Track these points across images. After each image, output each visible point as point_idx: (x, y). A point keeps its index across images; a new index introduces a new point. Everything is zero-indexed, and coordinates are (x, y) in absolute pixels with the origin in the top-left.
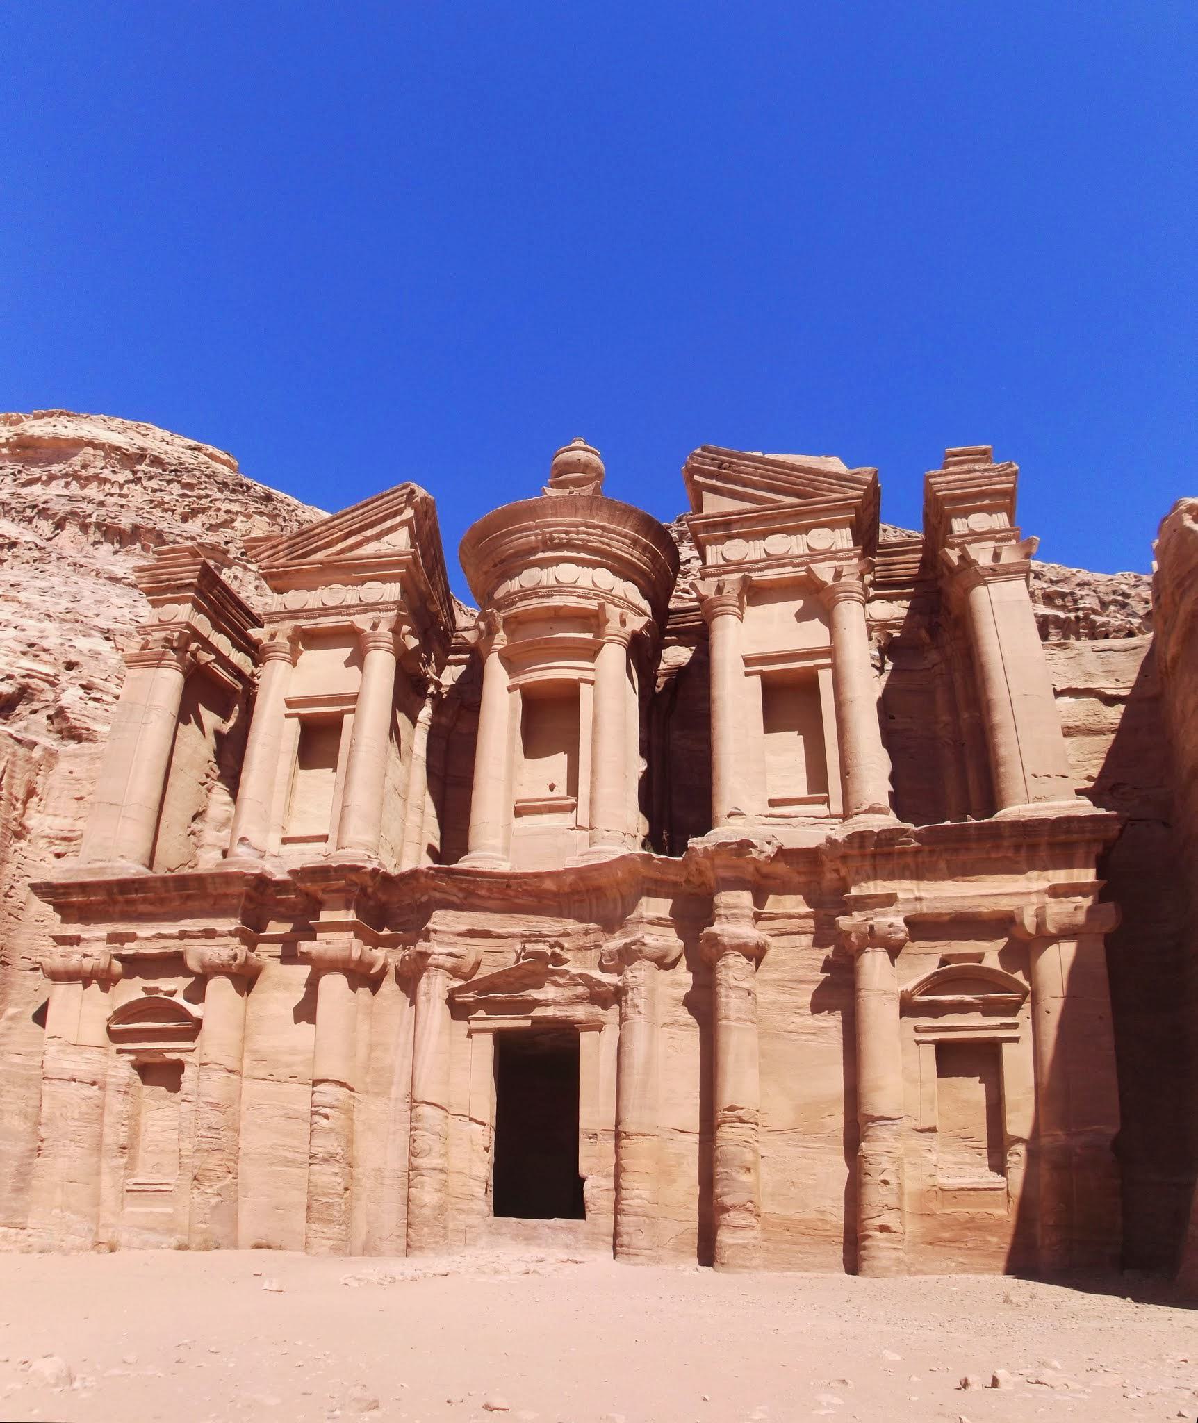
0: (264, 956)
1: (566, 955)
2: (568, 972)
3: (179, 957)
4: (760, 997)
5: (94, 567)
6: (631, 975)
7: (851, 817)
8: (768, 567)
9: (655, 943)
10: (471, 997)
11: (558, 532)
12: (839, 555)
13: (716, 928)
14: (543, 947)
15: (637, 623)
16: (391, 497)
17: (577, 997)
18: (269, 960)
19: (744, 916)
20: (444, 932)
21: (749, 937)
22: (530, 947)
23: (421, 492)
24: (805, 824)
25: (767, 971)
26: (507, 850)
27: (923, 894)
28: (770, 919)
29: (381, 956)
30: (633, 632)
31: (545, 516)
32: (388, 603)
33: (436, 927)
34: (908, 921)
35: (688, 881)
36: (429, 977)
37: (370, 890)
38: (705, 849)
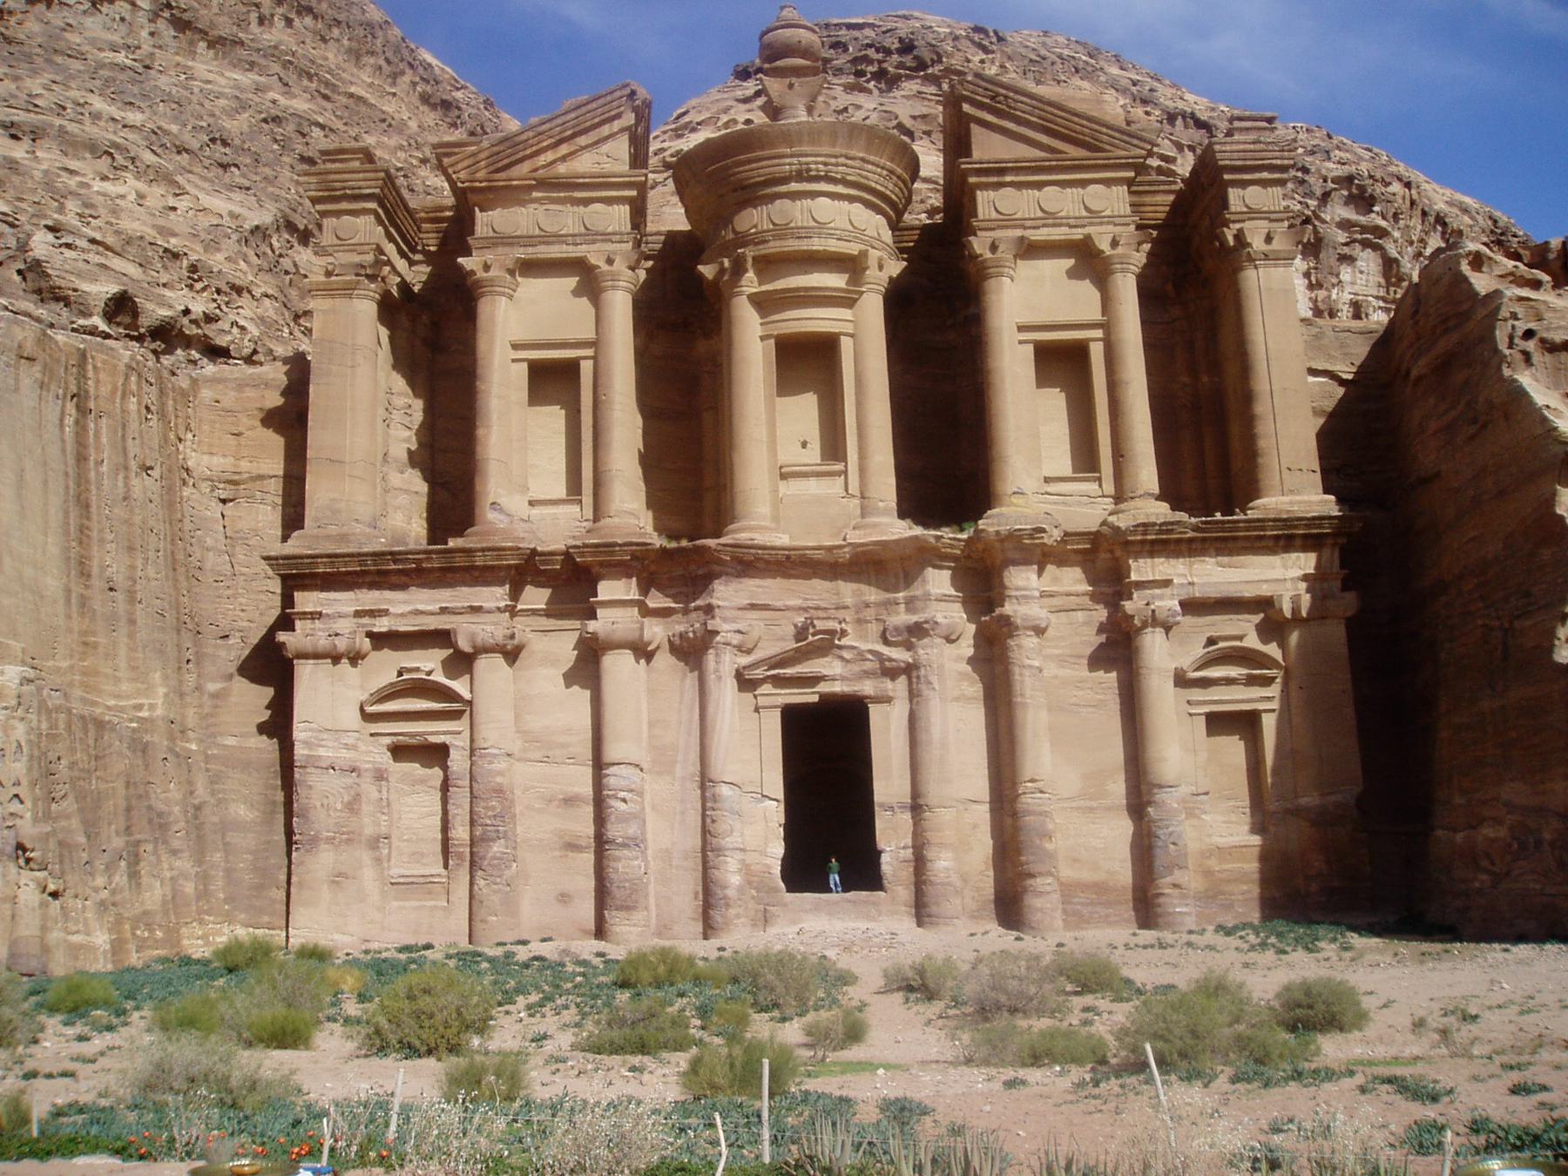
1: (849, 628)
2: (853, 648)
3: (441, 638)
4: (1046, 673)
7: (1126, 500)
8: (1044, 226)
10: (759, 673)
11: (816, 163)
12: (1117, 220)
13: (1008, 608)
15: (896, 267)
16: (609, 98)
17: (865, 672)
18: (530, 636)
19: (1033, 597)
20: (723, 607)
21: (1039, 619)
22: (820, 625)
23: (642, 93)
24: (1080, 504)
26: (776, 519)
27: (1195, 580)
29: (656, 632)
30: (891, 278)
31: (800, 143)
32: (621, 234)
33: (720, 603)
34: (1183, 604)
35: (968, 557)
36: (717, 655)
38: (998, 533)
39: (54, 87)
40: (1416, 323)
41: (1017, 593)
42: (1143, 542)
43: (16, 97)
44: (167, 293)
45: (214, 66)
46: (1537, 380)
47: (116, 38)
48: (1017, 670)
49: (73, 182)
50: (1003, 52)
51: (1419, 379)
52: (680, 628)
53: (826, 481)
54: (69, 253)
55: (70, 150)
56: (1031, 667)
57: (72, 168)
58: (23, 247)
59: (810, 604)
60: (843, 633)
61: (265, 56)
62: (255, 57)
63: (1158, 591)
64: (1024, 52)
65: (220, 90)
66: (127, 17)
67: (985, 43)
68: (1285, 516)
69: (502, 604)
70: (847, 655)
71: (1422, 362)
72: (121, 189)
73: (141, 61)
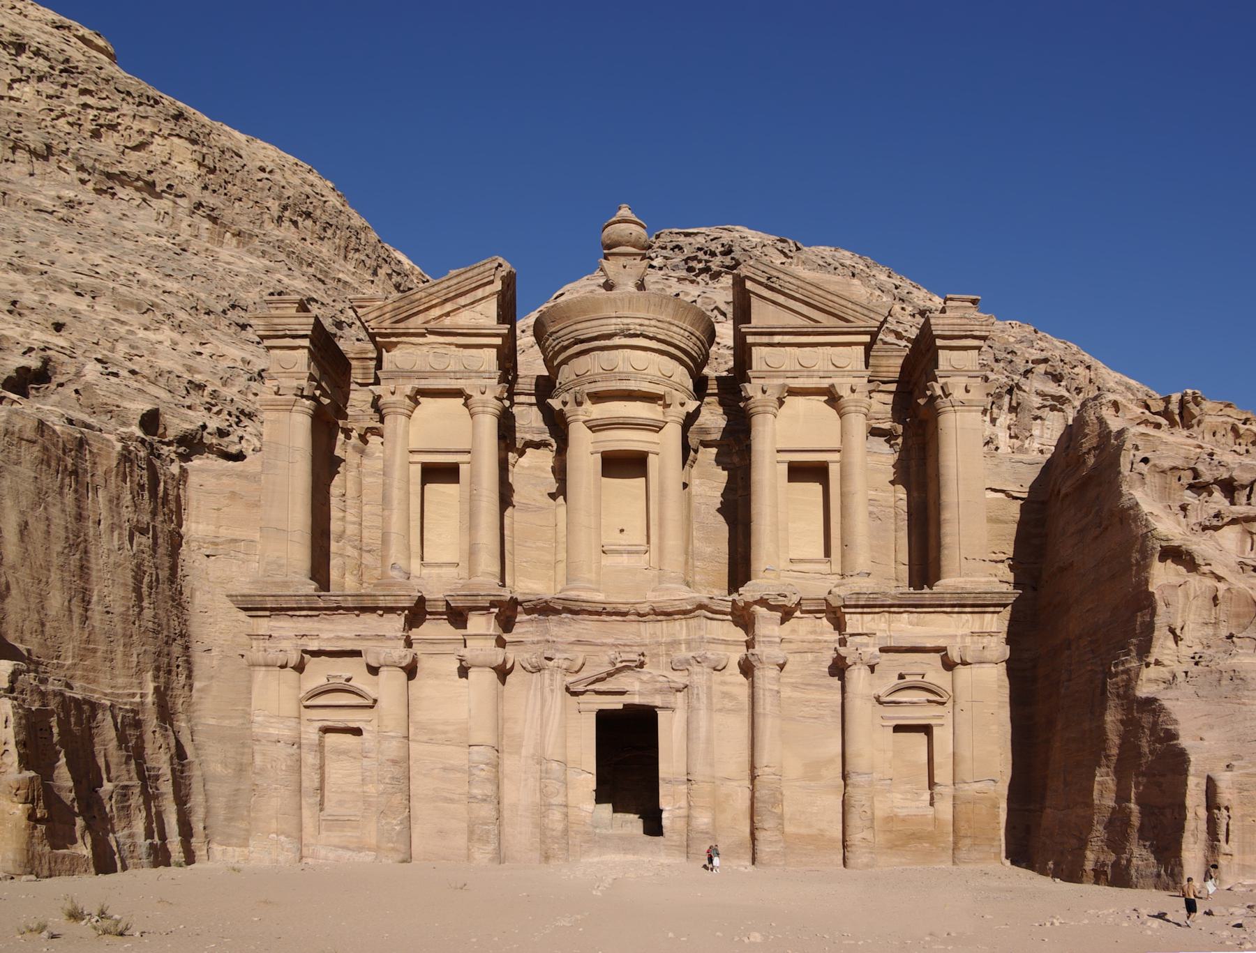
0: (418, 653)
1: (647, 660)
5: (20, 195)
6: (695, 677)
9: (713, 657)
10: (581, 688)
14: (634, 657)
17: (656, 690)
19: (775, 643)
20: (558, 642)
22: (625, 656)
24: (814, 579)
25: (786, 677)
27: (892, 634)
28: (790, 642)
33: (555, 639)
36: (552, 675)
37: (502, 609)
38: (752, 596)
39: (111, 260)
40: (1067, 455)
41: (764, 639)
42: (856, 606)
43: (81, 265)
44: (190, 412)
45: (235, 252)
46: (1147, 495)
47: (161, 227)
48: (761, 692)
49: (122, 330)
50: (798, 258)
51: (1067, 495)
52: (527, 656)
53: (635, 557)
54: (113, 379)
55: (121, 306)
56: (771, 690)
57: (122, 319)
58: (78, 374)
59: (620, 642)
60: (641, 665)
61: (274, 247)
62: (266, 247)
63: (864, 639)
64: (814, 258)
65: (238, 269)
66: (170, 212)
67: (786, 251)
68: (959, 591)
69: (399, 634)
70: (645, 678)
71: (1069, 483)
72: (159, 337)
73: (179, 245)
